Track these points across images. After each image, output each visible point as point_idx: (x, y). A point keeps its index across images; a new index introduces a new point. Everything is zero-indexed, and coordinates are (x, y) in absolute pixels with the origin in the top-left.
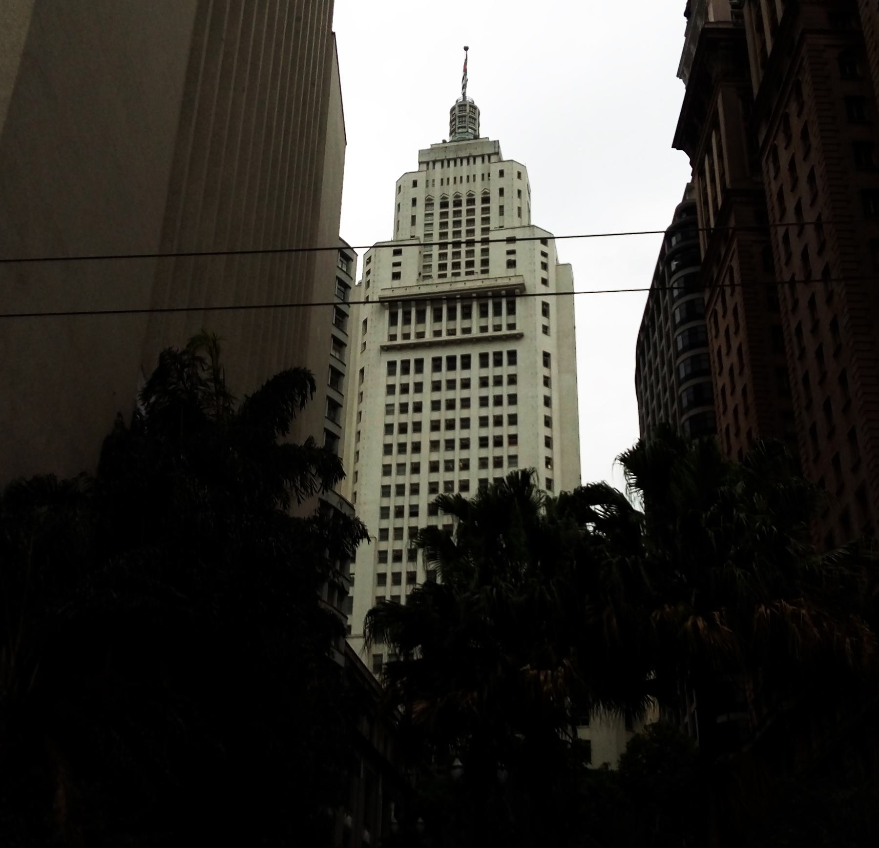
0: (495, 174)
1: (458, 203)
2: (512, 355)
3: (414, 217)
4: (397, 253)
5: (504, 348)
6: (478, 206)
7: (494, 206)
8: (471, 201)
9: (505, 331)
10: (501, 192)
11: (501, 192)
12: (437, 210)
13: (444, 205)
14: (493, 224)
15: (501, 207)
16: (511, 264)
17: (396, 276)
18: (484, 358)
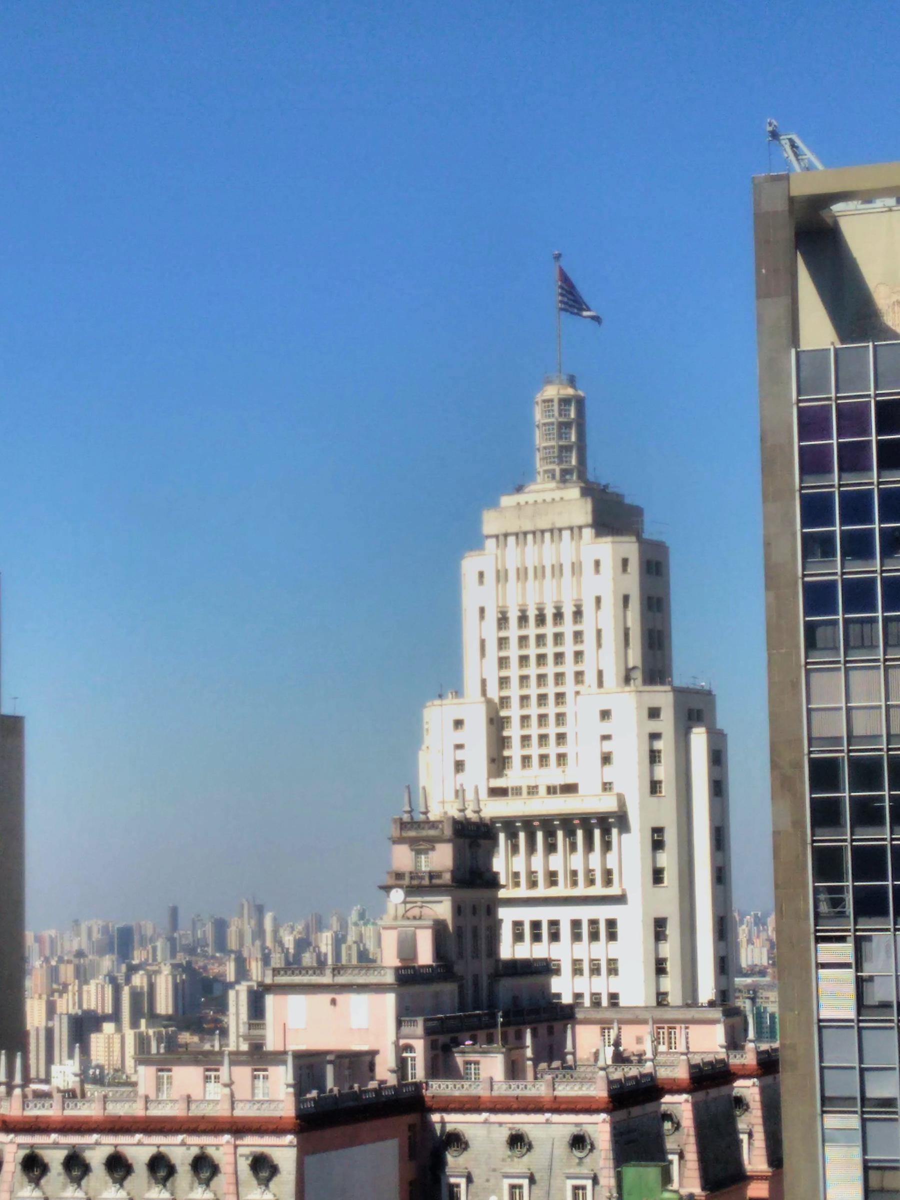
0: (588, 567)
1: (541, 619)
2: (611, 924)
3: (483, 643)
4: (458, 724)
5: (602, 913)
6: (568, 627)
7: (588, 626)
8: (558, 616)
9: (598, 890)
10: (598, 600)
11: (598, 600)
12: (513, 632)
13: (523, 619)
14: (589, 667)
15: (599, 632)
16: (606, 759)
17: (459, 766)
18: (576, 924)
